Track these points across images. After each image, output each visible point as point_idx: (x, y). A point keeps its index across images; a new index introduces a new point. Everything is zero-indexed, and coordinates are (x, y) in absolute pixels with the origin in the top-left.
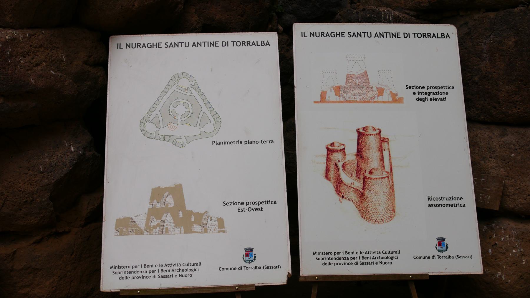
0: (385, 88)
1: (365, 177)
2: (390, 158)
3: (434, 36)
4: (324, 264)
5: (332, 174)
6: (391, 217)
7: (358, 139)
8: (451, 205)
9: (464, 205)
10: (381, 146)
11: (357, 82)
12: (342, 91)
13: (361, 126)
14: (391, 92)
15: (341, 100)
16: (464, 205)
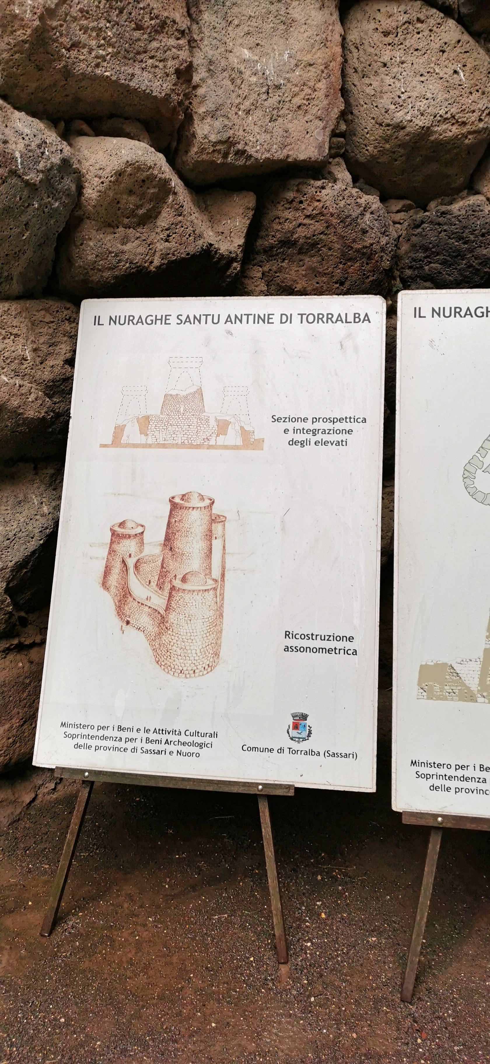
0: (232, 420)
1: (173, 588)
4: (78, 746)
5: (114, 579)
6: (211, 667)
7: (170, 517)
8: (329, 651)
9: (355, 653)
10: (210, 531)
11: (182, 410)
12: (152, 426)
14: (242, 428)
15: (150, 441)
16: (355, 653)
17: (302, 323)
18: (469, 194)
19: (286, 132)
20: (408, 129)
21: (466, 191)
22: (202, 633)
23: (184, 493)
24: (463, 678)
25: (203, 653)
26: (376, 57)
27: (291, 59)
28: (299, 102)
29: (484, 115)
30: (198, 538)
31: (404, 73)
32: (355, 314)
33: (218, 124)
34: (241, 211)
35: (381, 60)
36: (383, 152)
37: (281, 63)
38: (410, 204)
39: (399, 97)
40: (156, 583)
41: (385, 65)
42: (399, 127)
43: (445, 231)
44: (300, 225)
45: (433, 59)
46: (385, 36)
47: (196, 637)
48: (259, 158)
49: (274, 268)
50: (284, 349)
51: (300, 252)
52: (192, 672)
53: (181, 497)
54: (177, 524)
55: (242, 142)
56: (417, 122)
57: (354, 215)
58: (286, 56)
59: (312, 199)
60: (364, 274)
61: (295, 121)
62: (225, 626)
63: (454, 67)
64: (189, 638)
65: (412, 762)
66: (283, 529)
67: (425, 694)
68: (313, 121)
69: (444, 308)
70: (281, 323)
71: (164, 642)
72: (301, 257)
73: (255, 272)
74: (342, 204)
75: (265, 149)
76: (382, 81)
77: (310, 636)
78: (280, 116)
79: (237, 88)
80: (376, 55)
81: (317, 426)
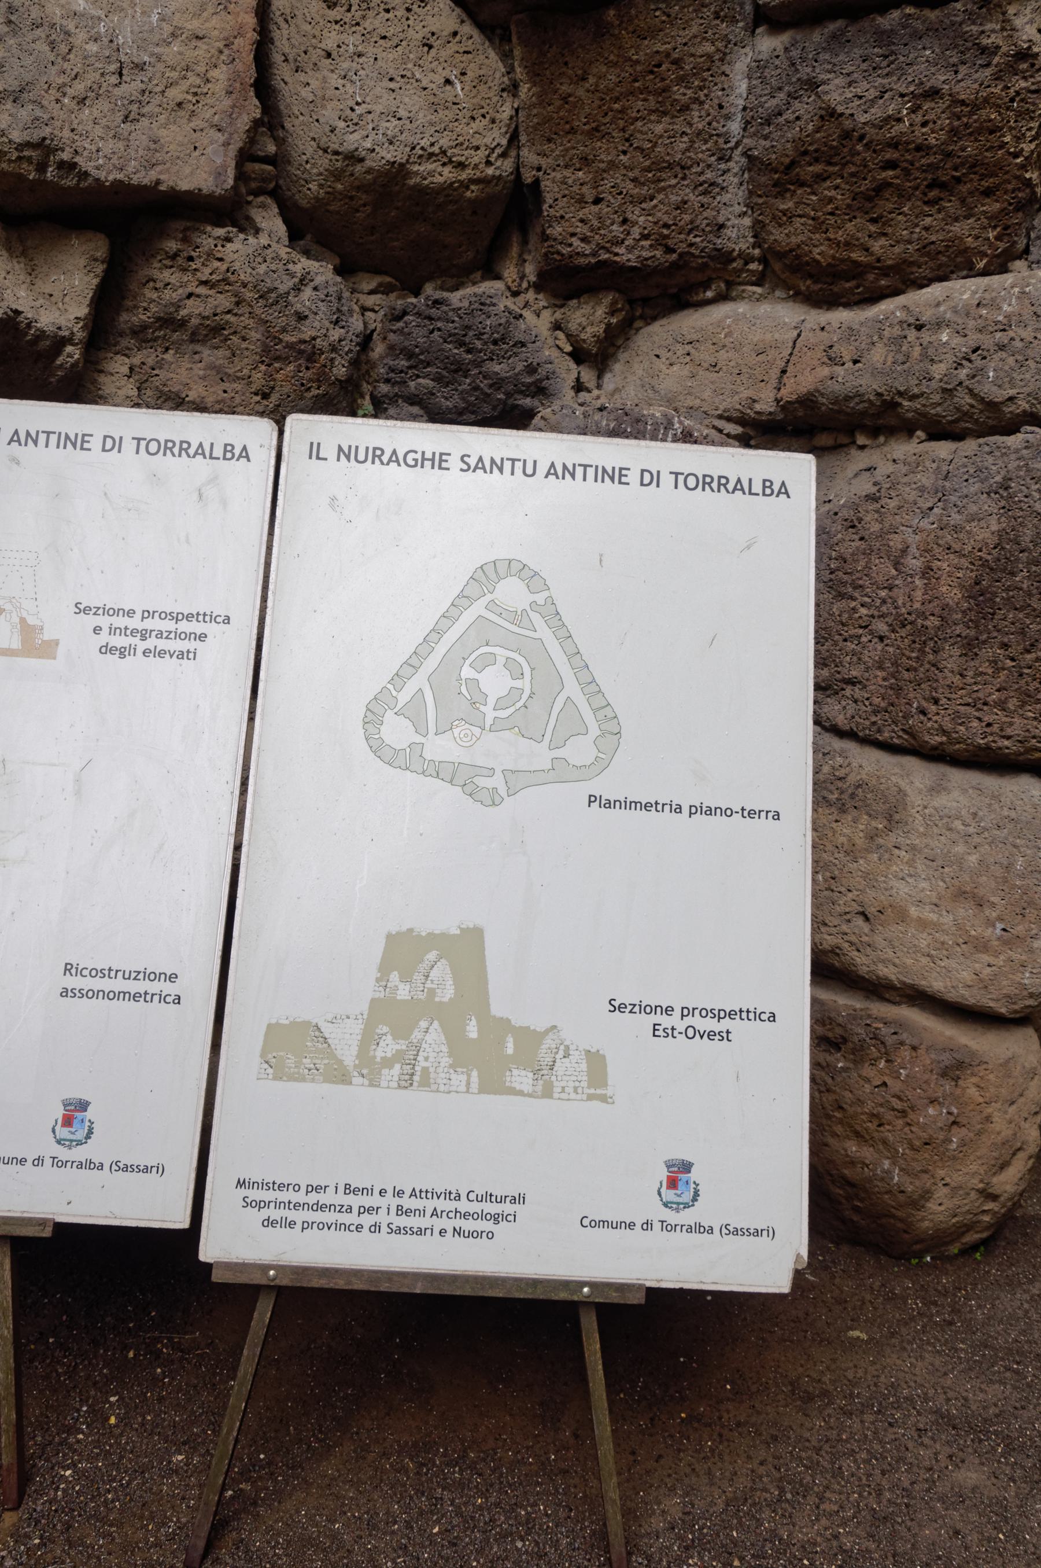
0: (8, 607)
3: (200, 450)
8: (135, 997)
16: (178, 1000)
17: (137, 452)
18: (484, 279)
19: (155, 142)
20: (368, 163)
21: (478, 275)
24: (333, 1046)
26: (314, 41)
27: (164, 24)
28: (180, 98)
29: (495, 155)
31: (361, 72)
32: (226, 445)
33: (24, 114)
34: (82, 262)
35: (323, 46)
36: (332, 194)
37: (146, 28)
38: (389, 283)
39: (352, 109)
41: (329, 55)
42: (353, 158)
43: (439, 329)
44: (190, 295)
45: (411, 56)
46: (329, 7)
48: (103, 179)
49: (150, 361)
50: (105, 494)
51: (194, 339)
55: (68, 149)
56: (384, 153)
57: (283, 288)
58: (155, 18)
59: (208, 255)
60: (302, 385)
61: (173, 128)
63: (446, 73)
65: (239, 1181)
66: (78, 793)
67: (270, 1071)
68: (205, 131)
69: (357, 447)
70: (104, 450)
72: (198, 347)
73: (117, 365)
74: (262, 269)
75: (114, 165)
76: (325, 80)
77: (106, 972)
78: (143, 115)
79: (60, 58)
80: (315, 37)
81: (149, 624)
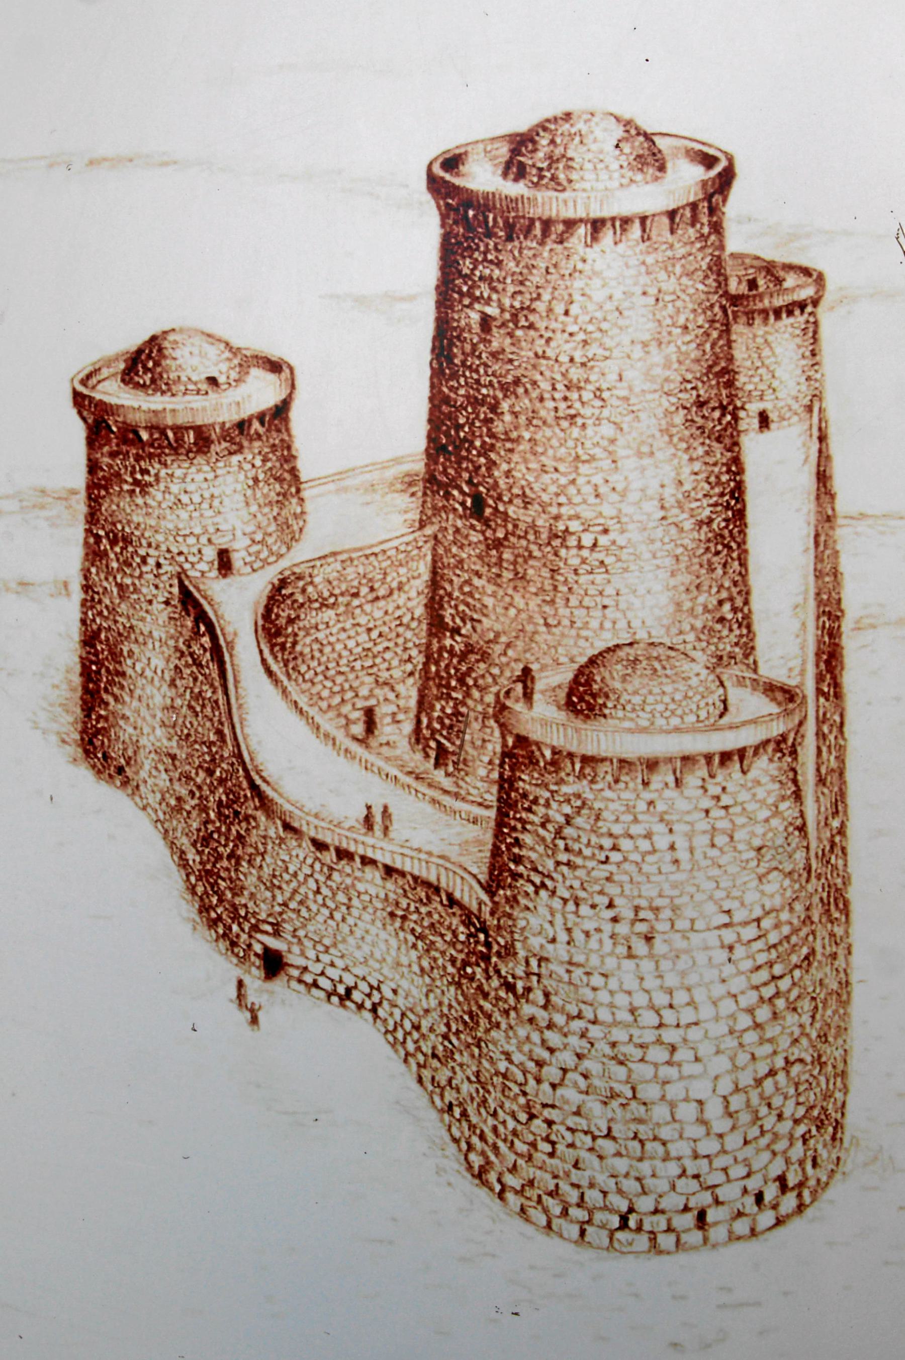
1: (519, 753)
2: (826, 519)
5: (147, 710)
6: (796, 1192)
7: (450, 289)
10: (724, 373)
13: (480, 117)
22: (727, 1006)
23: (522, 126)
25: (745, 1118)
30: (649, 423)
40: (408, 727)
47: (694, 1034)
52: (689, 1219)
53: (503, 151)
54: (498, 340)
62: (862, 964)
64: (649, 1036)
71: (502, 1066)
